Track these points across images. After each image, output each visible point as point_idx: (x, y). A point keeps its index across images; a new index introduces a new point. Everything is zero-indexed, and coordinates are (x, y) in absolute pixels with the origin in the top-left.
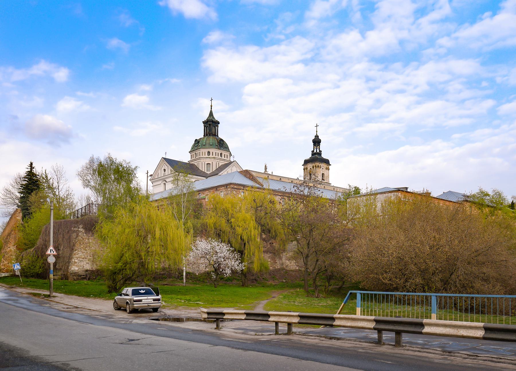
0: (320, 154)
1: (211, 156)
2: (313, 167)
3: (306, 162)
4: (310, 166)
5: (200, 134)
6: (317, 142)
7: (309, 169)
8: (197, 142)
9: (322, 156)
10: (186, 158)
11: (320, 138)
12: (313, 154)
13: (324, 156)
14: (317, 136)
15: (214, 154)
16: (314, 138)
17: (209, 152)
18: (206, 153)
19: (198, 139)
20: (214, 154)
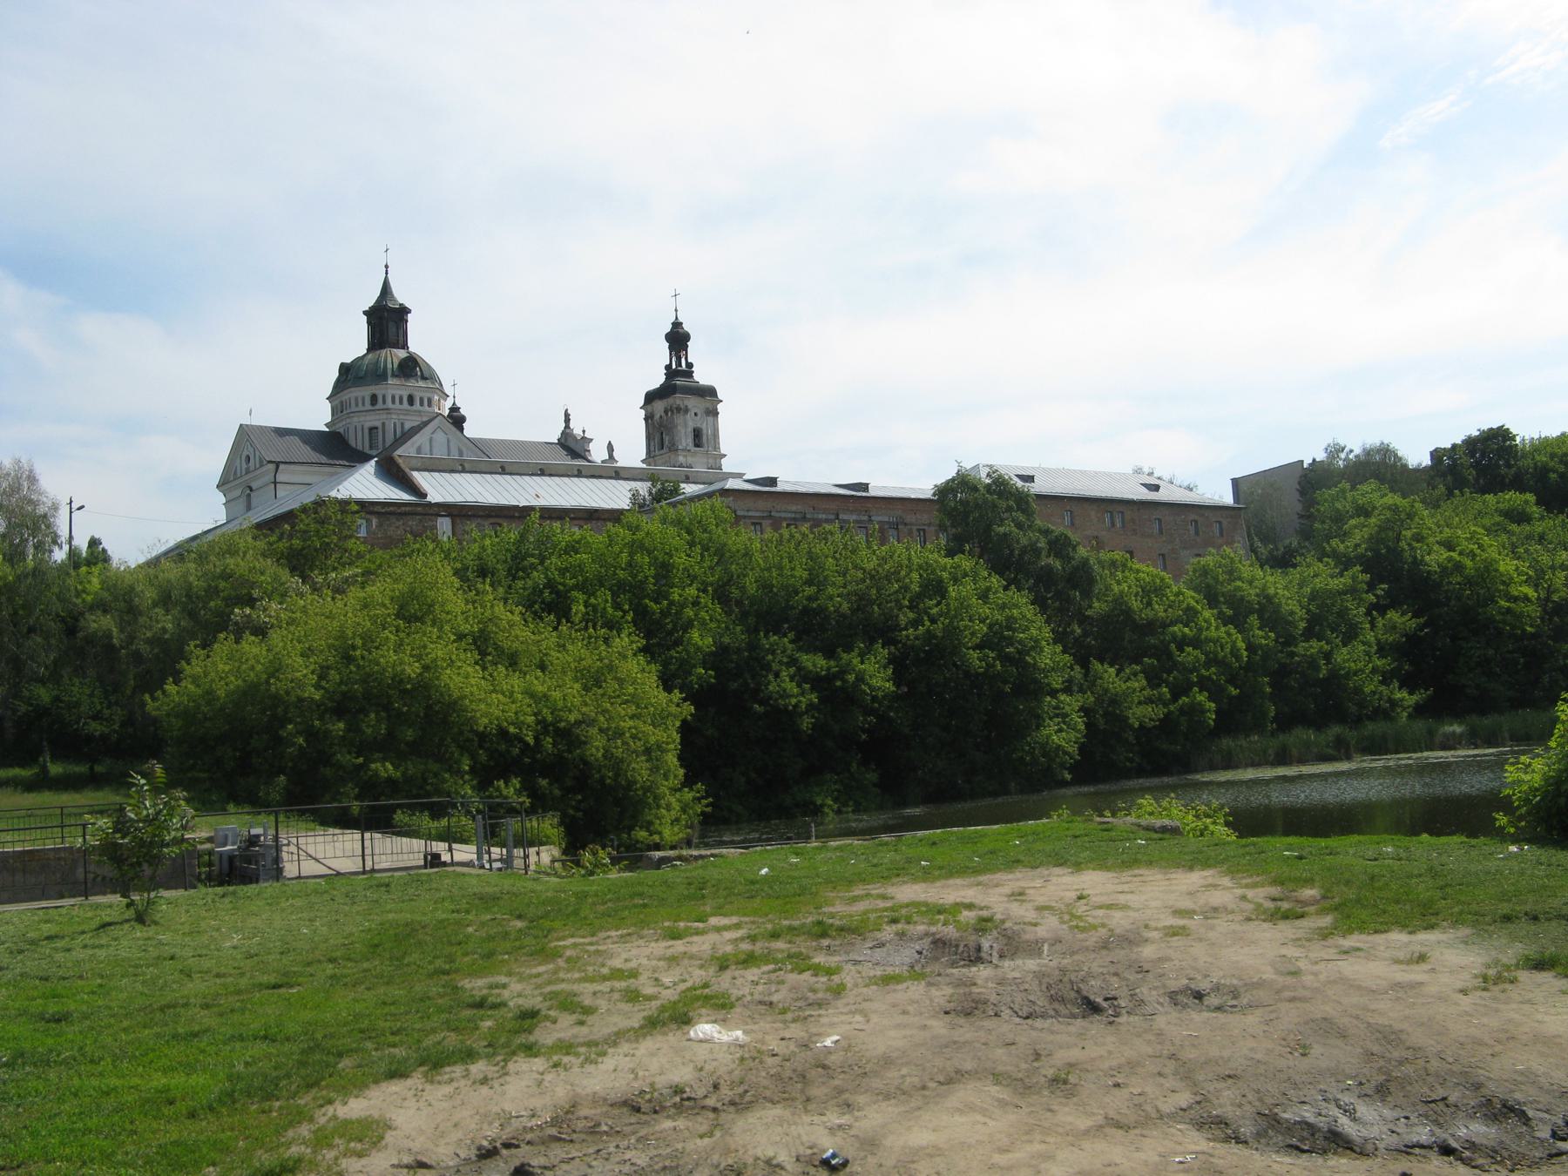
0: (688, 373)
1: (380, 405)
2: (666, 412)
3: (651, 397)
4: (659, 406)
5: (355, 344)
6: (678, 339)
7: (657, 417)
8: (344, 369)
9: (696, 376)
10: (318, 417)
11: (686, 327)
12: (671, 373)
13: (701, 376)
14: (677, 325)
15: (389, 400)
16: (668, 328)
17: (374, 399)
18: (368, 401)
19: (348, 360)
20: (389, 400)
